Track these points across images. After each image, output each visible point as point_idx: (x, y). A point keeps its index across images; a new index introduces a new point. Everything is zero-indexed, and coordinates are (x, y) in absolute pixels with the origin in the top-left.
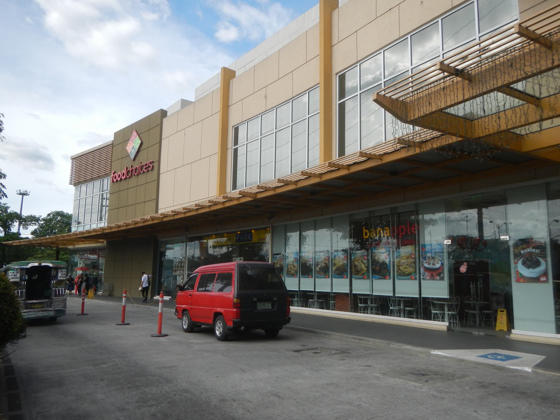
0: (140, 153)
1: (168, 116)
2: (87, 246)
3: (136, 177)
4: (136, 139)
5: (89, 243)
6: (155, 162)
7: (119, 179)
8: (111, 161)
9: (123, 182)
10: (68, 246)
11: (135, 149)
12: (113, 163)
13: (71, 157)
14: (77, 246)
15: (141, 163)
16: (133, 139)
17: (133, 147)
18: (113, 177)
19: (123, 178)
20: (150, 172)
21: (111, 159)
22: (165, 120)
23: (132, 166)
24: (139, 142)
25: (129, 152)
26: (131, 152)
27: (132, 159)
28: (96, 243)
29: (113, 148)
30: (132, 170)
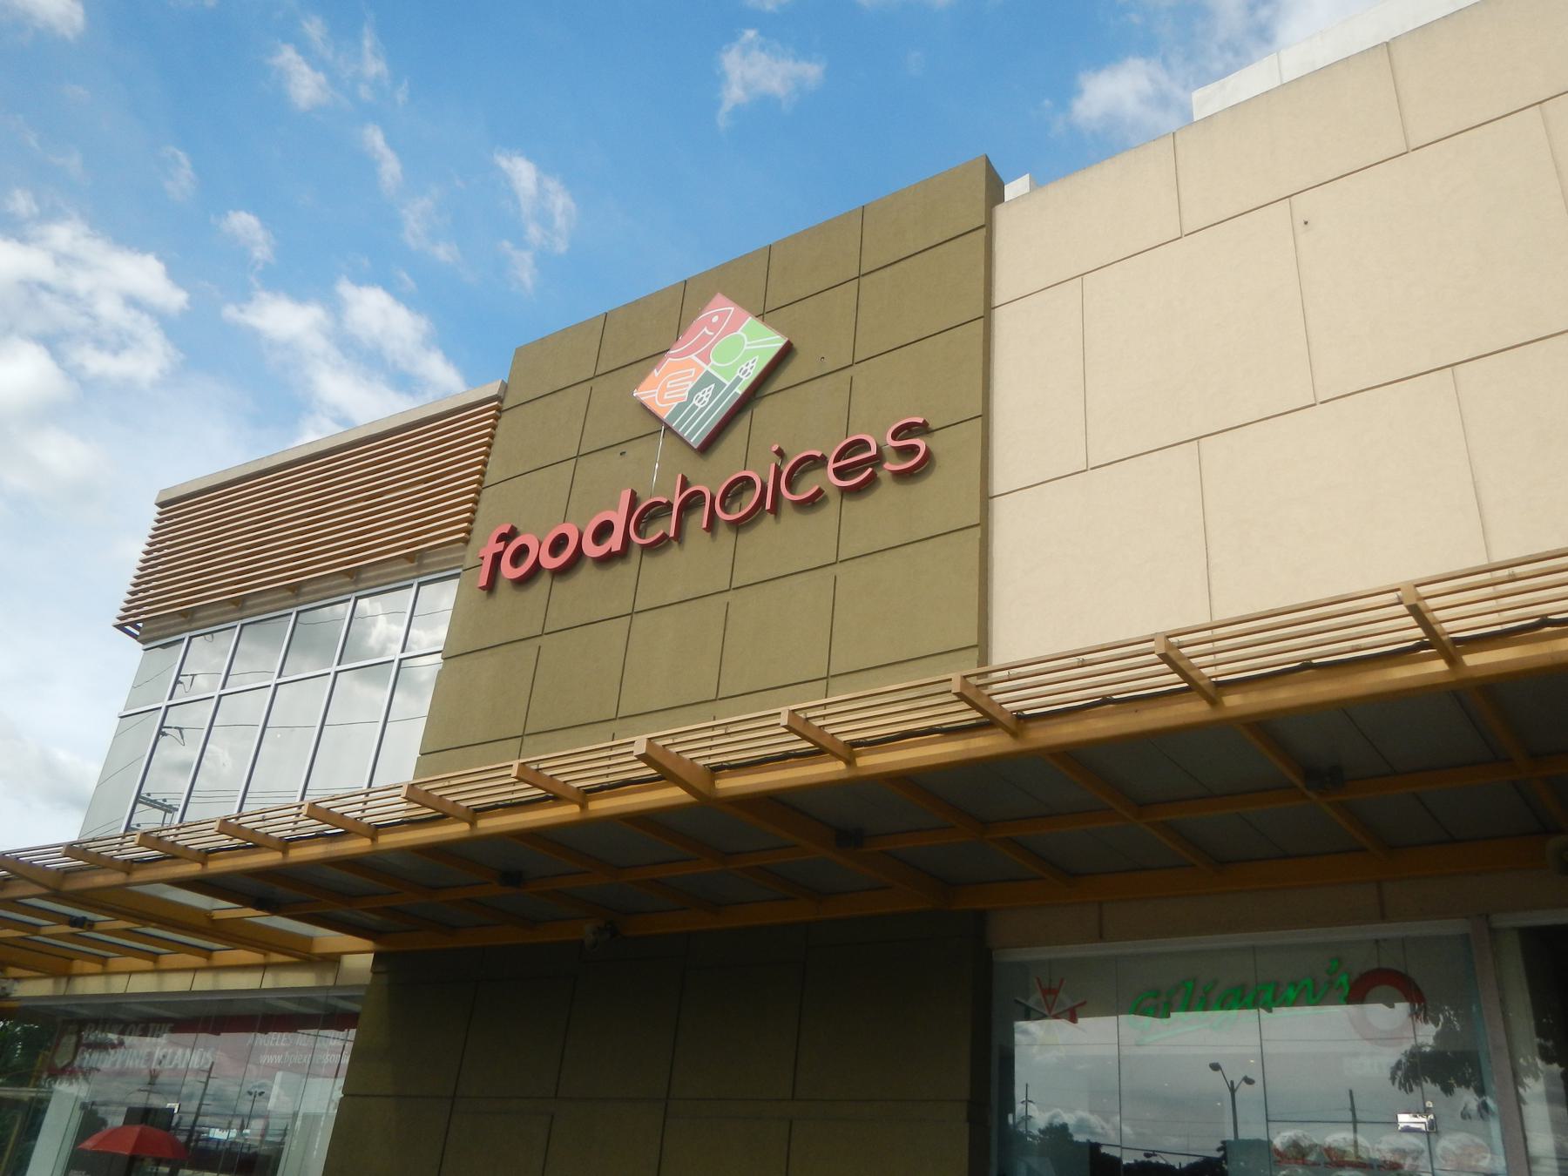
0: (763, 411)
1: (1006, 200)
2: (176, 983)
3: (725, 537)
4: (739, 332)
5: (195, 970)
6: (933, 425)
7: (549, 563)
8: (480, 482)
9: (586, 576)
10: (18, 979)
11: (720, 385)
12: (486, 494)
13: (162, 492)
14: (92, 986)
15: (780, 453)
16: (705, 338)
17: (708, 379)
18: (497, 558)
19: (592, 550)
20: (888, 494)
21: (482, 473)
22: (1000, 211)
23: (685, 484)
24: (773, 343)
25: (664, 409)
26: (681, 407)
27: (696, 440)
28: (264, 967)
29: (497, 418)
30: (692, 503)
